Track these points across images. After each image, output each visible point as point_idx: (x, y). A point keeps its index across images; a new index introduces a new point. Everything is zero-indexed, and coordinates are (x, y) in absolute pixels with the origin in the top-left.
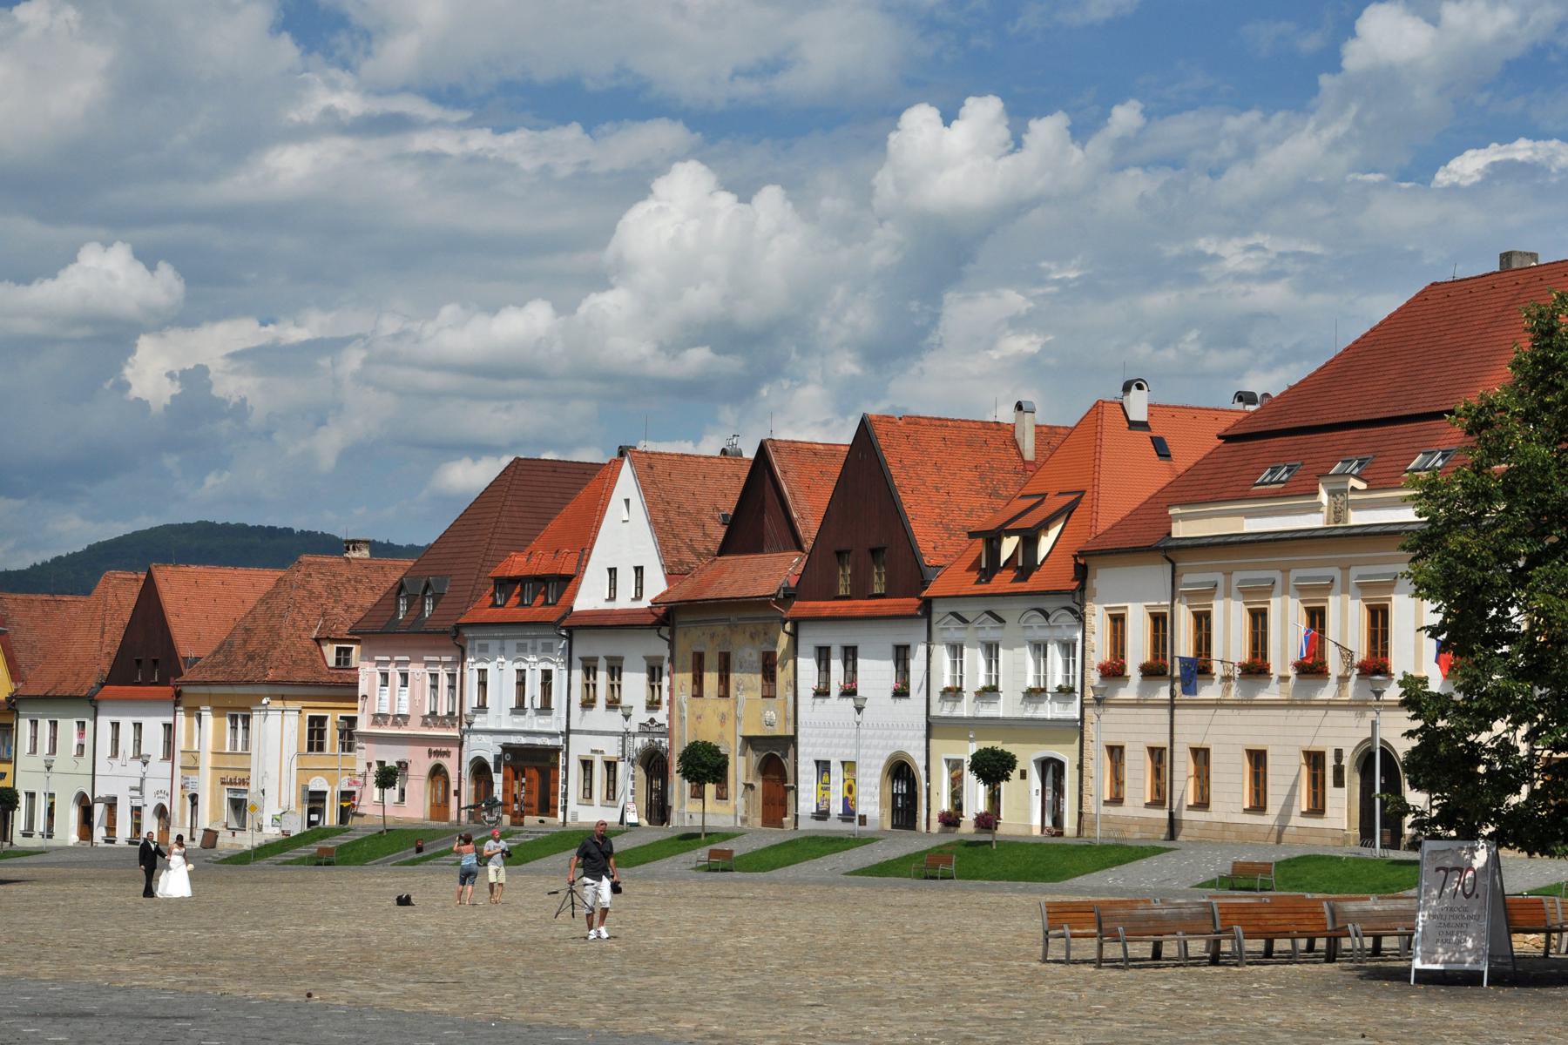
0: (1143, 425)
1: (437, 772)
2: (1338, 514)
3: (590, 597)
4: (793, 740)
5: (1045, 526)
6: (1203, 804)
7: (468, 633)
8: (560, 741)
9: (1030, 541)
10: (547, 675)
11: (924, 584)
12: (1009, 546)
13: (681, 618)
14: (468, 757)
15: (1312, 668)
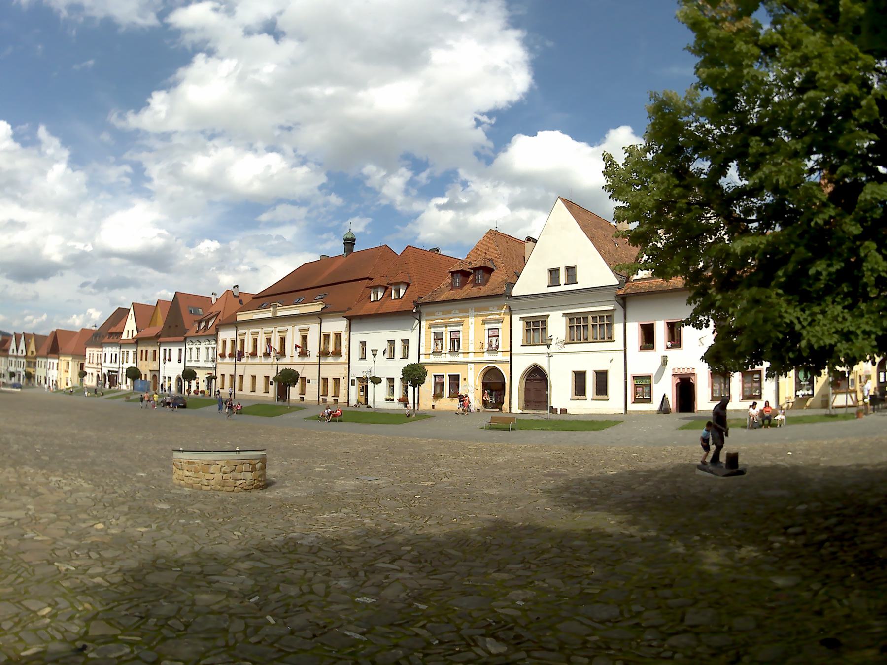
1: (98, 375)
3: (124, 337)
5: (211, 319)
8: (117, 370)
9: (207, 323)
10: (116, 354)
11: (185, 333)
12: (203, 324)
13: (139, 342)
15: (267, 355)
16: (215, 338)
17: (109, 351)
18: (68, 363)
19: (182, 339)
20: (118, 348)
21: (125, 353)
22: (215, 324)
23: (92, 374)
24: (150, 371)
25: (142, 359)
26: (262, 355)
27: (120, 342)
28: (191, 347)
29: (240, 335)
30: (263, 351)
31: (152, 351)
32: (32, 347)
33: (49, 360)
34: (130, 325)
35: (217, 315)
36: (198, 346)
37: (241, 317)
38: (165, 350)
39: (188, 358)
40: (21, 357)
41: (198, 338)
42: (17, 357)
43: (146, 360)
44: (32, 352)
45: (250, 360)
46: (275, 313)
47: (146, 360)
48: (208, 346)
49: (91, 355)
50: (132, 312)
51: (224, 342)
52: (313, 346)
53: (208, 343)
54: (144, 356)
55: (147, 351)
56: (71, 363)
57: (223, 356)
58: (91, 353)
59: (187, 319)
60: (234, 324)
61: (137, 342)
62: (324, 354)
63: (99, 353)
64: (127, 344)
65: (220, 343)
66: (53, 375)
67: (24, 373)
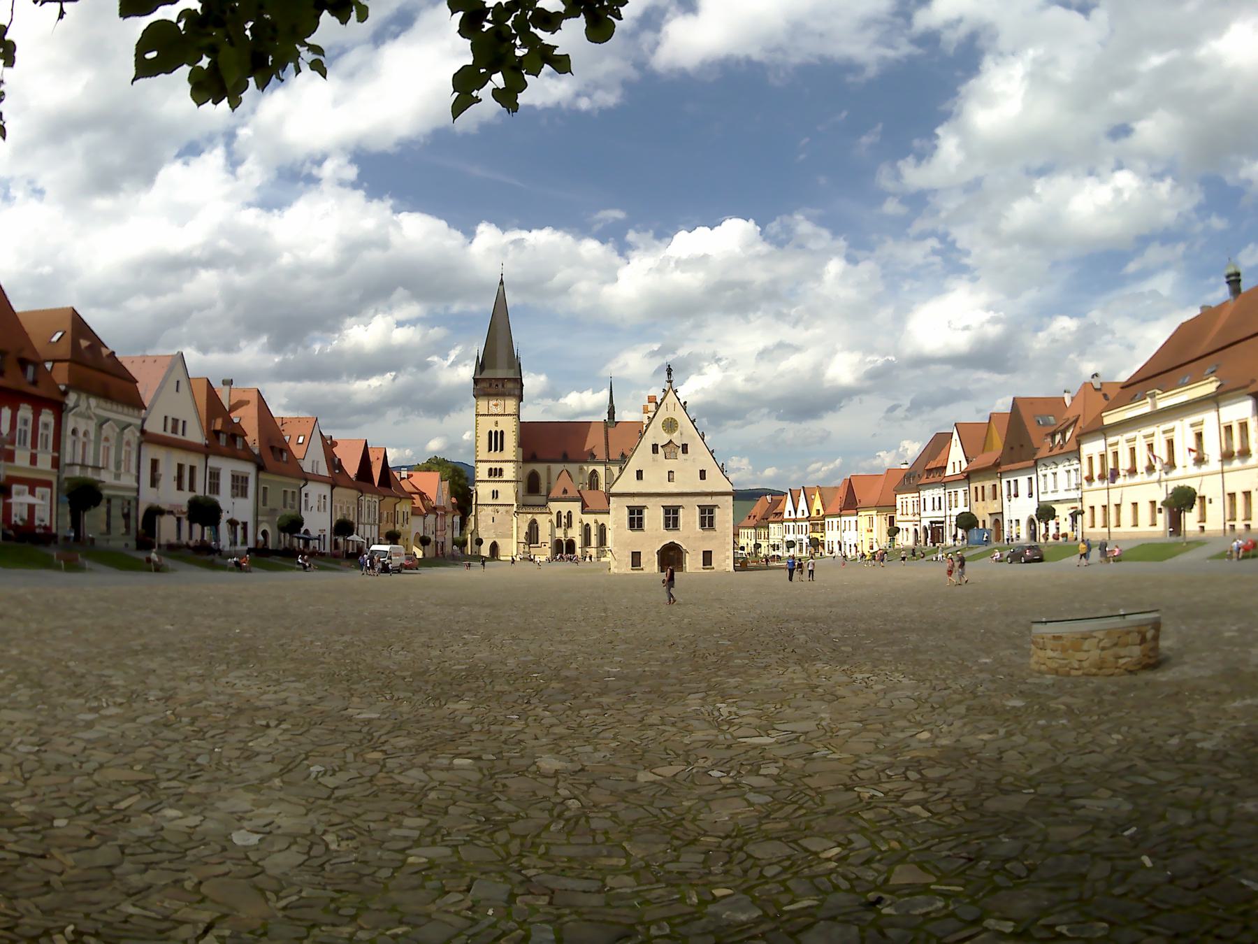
0: (1100, 390)
1: (916, 530)
2: (1154, 405)
3: (949, 472)
4: (1002, 513)
5: (1067, 428)
6: (1118, 526)
7: (920, 487)
8: (943, 519)
9: (1064, 433)
10: (940, 498)
11: (1035, 454)
12: (1058, 437)
13: (971, 476)
14: (922, 526)
15: (1150, 469)
16: (1077, 454)
17: (928, 494)
18: (871, 519)
19: (1031, 463)
20: (942, 489)
21: (953, 494)
22: (1074, 435)
23: (907, 530)
24: (990, 514)
25: (977, 500)
26: (1144, 471)
27: (944, 480)
28: (1044, 472)
29: (1111, 445)
30: (1146, 463)
31: (991, 487)
32: (817, 504)
33: (843, 519)
34: (956, 458)
35: (1076, 421)
36: (1054, 470)
37: (1110, 419)
38: (1009, 482)
39: (1041, 489)
40: (802, 520)
41: (1054, 459)
42: (795, 521)
43: (983, 500)
44: (818, 511)
45: (1129, 480)
46: (1154, 405)
47: (983, 500)
48: (1068, 468)
49: (904, 504)
50: (955, 436)
51: (1090, 459)
52: (1212, 449)
53: (1067, 463)
54: (980, 496)
55: (983, 487)
56: (875, 517)
57: (1090, 479)
58: (904, 500)
59: (1035, 433)
60: (1103, 431)
61: (968, 476)
62: (1227, 456)
63: (915, 499)
64: (954, 481)
65: (1085, 460)
66: (850, 537)
67: (808, 541)
